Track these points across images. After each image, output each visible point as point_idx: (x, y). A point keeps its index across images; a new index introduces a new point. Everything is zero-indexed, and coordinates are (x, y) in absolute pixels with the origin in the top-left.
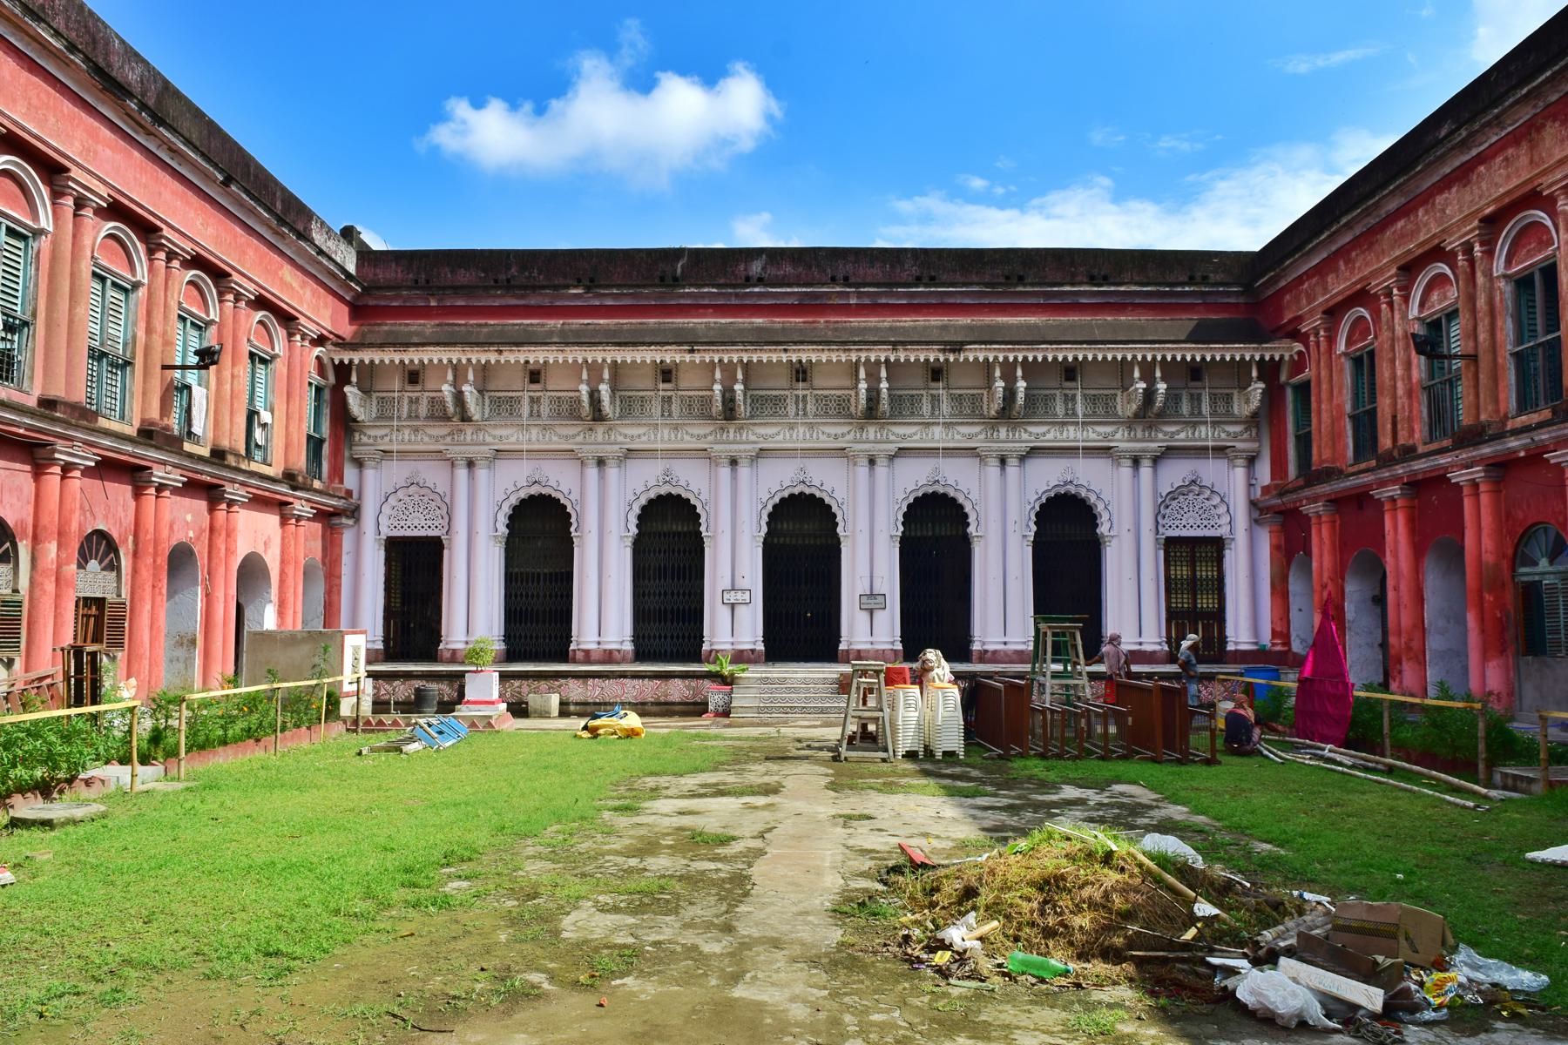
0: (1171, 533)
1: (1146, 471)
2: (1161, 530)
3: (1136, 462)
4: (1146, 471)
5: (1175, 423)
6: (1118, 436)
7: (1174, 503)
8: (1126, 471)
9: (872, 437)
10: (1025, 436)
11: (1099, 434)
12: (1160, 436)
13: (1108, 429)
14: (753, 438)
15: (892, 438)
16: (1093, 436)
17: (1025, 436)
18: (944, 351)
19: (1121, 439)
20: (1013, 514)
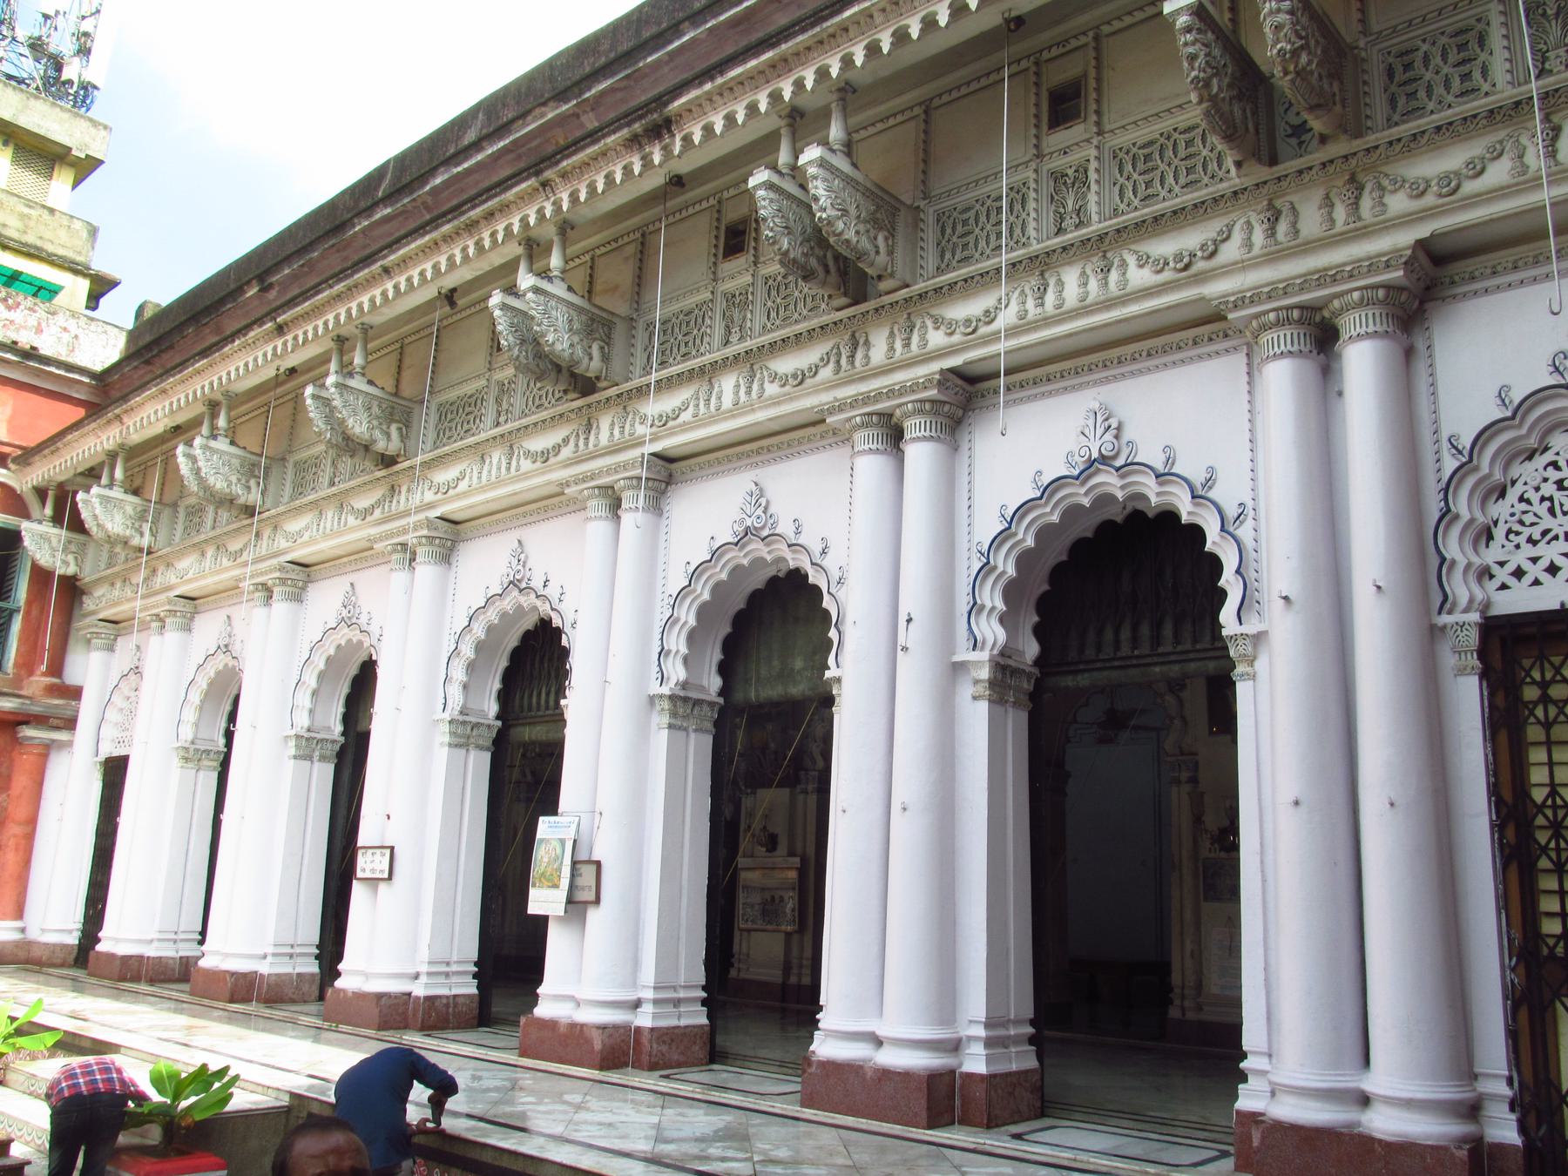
0: (1520, 600)
1: (1362, 362)
2: (1461, 589)
3: (1323, 338)
4: (1362, 362)
5: (1447, 133)
6: (1231, 251)
7: (1529, 472)
8: (1282, 378)
9: (604, 439)
10: (937, 338)
11: (1161, 265)
12: (1398, 203)
13: (1191, 239)
14: (429, 496)
15: (641, 430)
16: (1139, 276)
17: (937, 338)
18: (634, 142)
19: (1241, 261)
20: (915, 595)
